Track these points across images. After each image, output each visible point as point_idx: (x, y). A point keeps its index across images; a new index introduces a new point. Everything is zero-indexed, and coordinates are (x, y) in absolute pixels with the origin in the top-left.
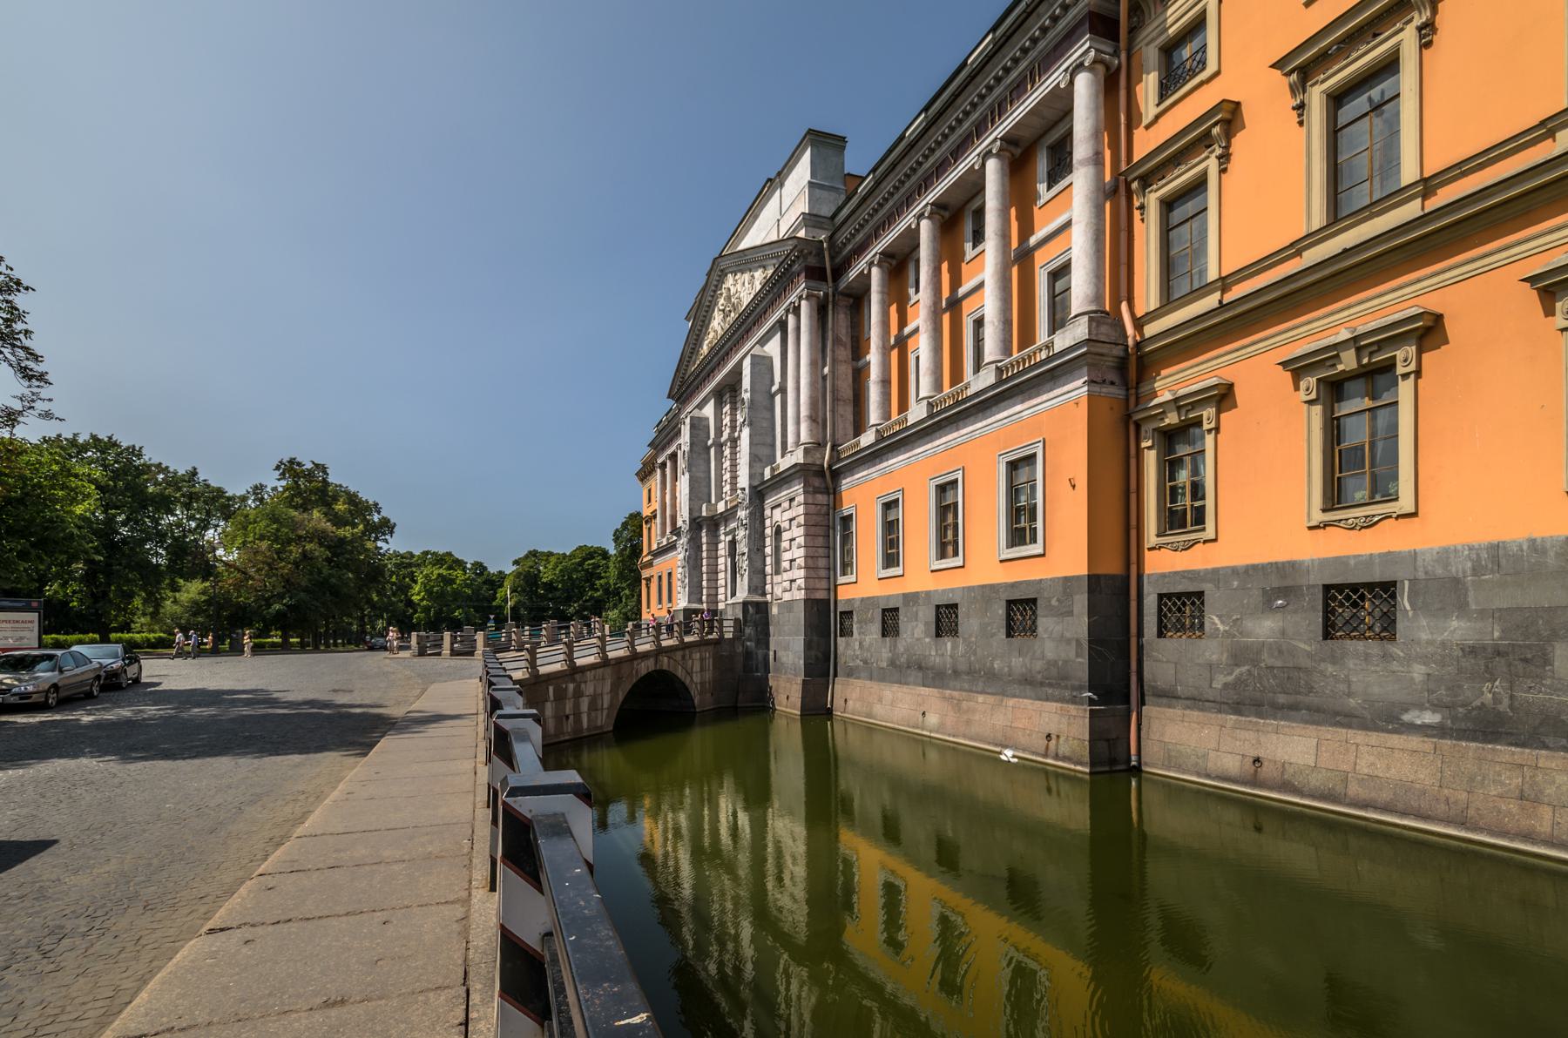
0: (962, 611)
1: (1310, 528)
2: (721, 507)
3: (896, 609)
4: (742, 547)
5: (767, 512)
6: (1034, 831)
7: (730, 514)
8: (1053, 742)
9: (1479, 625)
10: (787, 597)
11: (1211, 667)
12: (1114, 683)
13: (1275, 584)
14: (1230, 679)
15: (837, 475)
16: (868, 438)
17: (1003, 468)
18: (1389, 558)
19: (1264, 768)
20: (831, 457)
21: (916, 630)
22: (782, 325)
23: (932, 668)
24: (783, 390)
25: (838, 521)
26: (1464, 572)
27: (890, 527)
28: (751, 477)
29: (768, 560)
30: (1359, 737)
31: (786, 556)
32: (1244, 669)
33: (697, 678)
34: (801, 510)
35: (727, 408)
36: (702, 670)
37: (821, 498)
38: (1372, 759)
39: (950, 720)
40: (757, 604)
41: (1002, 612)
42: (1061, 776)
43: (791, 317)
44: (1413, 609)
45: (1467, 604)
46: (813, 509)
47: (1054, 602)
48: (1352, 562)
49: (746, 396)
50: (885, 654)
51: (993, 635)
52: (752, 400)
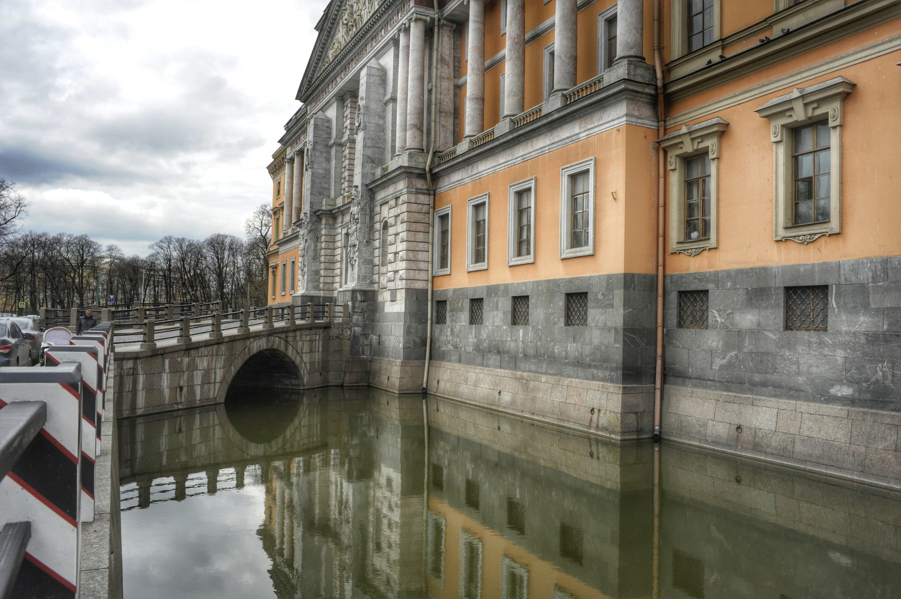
0: (532, 301)
1: (777, 241)
2: (339, 202)
3: (481, 300)
4: (353, 240)
5: (377, 209)
6: (579, 490)
7: (343, 211)
8: (596, 415)
9: (876, 319)
10: (391, 285)
11: (712, 352)
12: (645, 365)
13: (755, 287)
14: (724, 361)
15: (435, 178)
16: (463, 147)
17: (565, 182)
18: (825, 268)
19: (744, 434)
20: (432, 161)
21: (496, 317)
22: (395, 41)
23: (508, 352)
24: (394, 100)
25: (437, 220)
26: (868, 280)
27: (479, 225)
28: (364, 176)
29: (377, 253)
30: (804, 406)
31: (391, 249)
32: (733, 353)
33: (306, 358)
34: (404, 208)
35: (348, 112)
36: (311, 352)
37: (423, 199)
38: (811, 423)
39: (521, 396)
40: (364, 293)
41: (561, 303)
42: (600, 441)
43: (402, 35)
44: (838, 308)
45: (869, 304)
46: (415, 207)
47: (600, 297)
48: (802, 270)
49: (361, 103)
50: (472, 339)
51: (555, 323)
52: (367, 107)
